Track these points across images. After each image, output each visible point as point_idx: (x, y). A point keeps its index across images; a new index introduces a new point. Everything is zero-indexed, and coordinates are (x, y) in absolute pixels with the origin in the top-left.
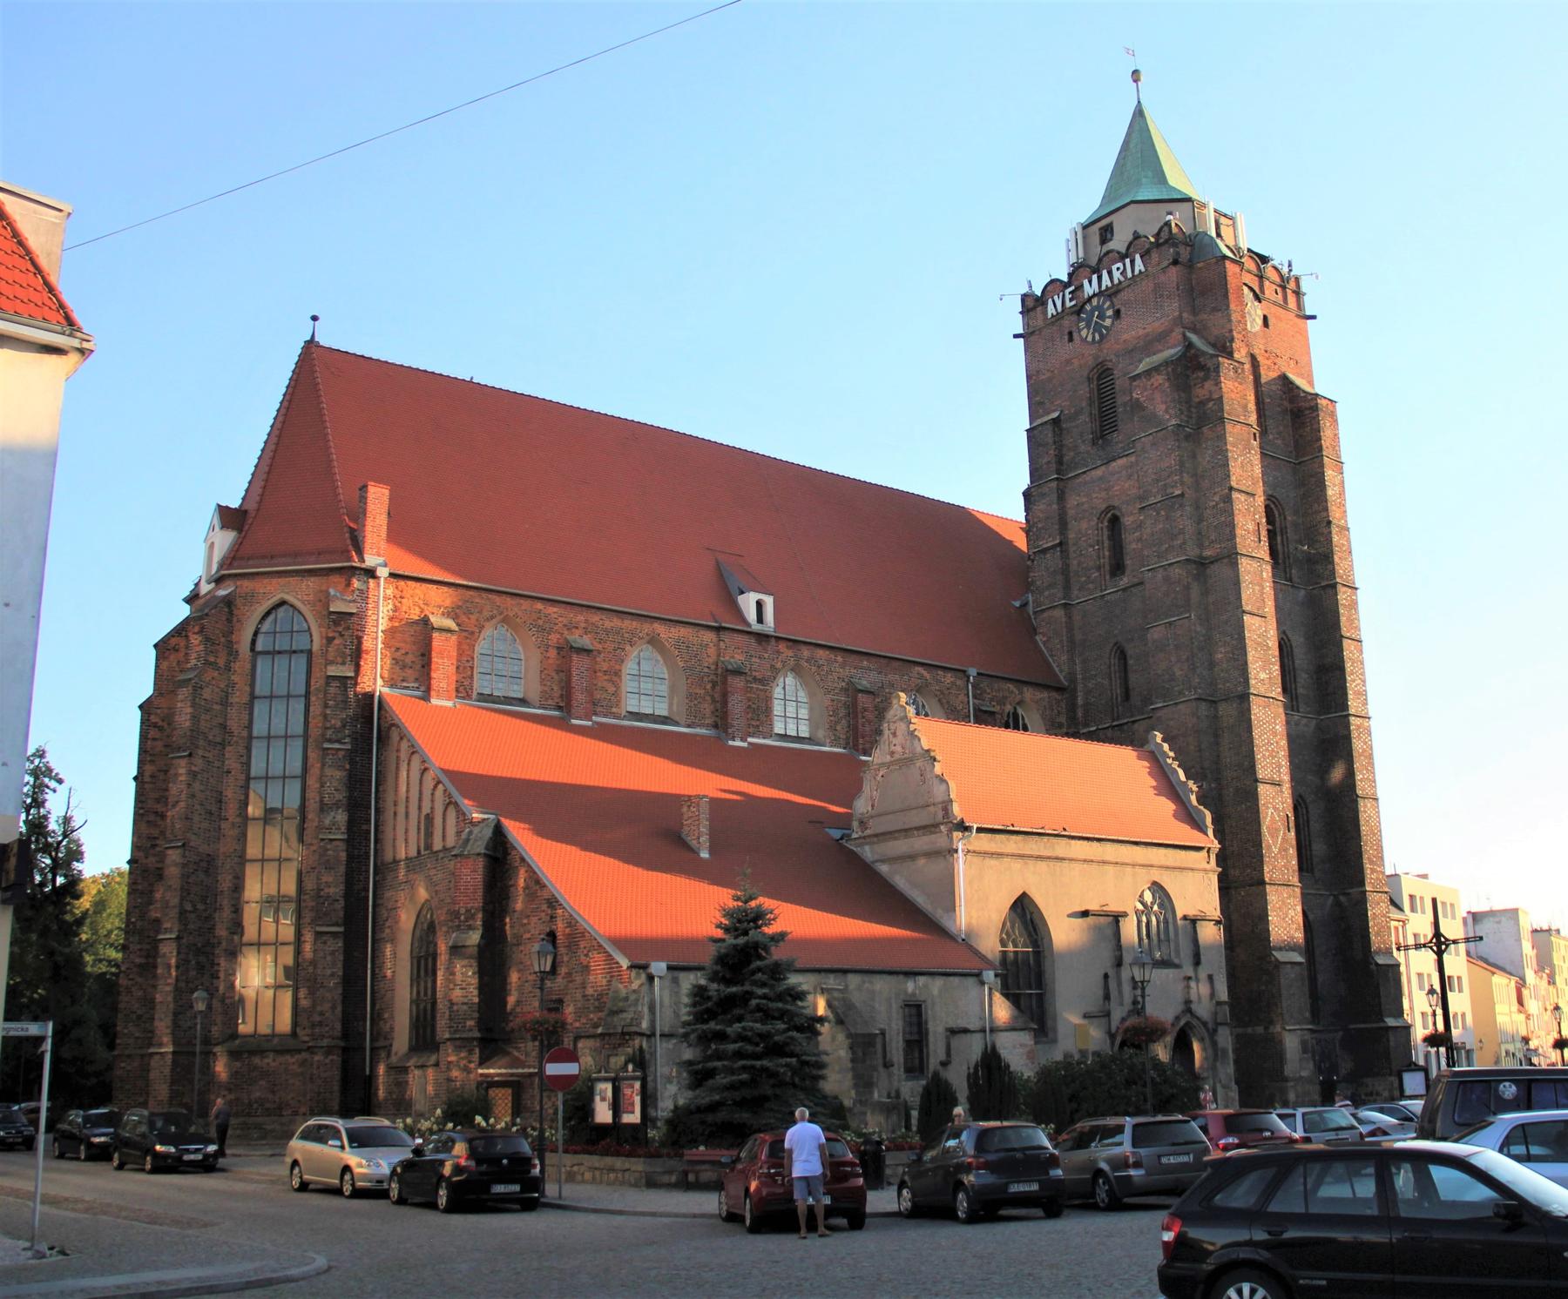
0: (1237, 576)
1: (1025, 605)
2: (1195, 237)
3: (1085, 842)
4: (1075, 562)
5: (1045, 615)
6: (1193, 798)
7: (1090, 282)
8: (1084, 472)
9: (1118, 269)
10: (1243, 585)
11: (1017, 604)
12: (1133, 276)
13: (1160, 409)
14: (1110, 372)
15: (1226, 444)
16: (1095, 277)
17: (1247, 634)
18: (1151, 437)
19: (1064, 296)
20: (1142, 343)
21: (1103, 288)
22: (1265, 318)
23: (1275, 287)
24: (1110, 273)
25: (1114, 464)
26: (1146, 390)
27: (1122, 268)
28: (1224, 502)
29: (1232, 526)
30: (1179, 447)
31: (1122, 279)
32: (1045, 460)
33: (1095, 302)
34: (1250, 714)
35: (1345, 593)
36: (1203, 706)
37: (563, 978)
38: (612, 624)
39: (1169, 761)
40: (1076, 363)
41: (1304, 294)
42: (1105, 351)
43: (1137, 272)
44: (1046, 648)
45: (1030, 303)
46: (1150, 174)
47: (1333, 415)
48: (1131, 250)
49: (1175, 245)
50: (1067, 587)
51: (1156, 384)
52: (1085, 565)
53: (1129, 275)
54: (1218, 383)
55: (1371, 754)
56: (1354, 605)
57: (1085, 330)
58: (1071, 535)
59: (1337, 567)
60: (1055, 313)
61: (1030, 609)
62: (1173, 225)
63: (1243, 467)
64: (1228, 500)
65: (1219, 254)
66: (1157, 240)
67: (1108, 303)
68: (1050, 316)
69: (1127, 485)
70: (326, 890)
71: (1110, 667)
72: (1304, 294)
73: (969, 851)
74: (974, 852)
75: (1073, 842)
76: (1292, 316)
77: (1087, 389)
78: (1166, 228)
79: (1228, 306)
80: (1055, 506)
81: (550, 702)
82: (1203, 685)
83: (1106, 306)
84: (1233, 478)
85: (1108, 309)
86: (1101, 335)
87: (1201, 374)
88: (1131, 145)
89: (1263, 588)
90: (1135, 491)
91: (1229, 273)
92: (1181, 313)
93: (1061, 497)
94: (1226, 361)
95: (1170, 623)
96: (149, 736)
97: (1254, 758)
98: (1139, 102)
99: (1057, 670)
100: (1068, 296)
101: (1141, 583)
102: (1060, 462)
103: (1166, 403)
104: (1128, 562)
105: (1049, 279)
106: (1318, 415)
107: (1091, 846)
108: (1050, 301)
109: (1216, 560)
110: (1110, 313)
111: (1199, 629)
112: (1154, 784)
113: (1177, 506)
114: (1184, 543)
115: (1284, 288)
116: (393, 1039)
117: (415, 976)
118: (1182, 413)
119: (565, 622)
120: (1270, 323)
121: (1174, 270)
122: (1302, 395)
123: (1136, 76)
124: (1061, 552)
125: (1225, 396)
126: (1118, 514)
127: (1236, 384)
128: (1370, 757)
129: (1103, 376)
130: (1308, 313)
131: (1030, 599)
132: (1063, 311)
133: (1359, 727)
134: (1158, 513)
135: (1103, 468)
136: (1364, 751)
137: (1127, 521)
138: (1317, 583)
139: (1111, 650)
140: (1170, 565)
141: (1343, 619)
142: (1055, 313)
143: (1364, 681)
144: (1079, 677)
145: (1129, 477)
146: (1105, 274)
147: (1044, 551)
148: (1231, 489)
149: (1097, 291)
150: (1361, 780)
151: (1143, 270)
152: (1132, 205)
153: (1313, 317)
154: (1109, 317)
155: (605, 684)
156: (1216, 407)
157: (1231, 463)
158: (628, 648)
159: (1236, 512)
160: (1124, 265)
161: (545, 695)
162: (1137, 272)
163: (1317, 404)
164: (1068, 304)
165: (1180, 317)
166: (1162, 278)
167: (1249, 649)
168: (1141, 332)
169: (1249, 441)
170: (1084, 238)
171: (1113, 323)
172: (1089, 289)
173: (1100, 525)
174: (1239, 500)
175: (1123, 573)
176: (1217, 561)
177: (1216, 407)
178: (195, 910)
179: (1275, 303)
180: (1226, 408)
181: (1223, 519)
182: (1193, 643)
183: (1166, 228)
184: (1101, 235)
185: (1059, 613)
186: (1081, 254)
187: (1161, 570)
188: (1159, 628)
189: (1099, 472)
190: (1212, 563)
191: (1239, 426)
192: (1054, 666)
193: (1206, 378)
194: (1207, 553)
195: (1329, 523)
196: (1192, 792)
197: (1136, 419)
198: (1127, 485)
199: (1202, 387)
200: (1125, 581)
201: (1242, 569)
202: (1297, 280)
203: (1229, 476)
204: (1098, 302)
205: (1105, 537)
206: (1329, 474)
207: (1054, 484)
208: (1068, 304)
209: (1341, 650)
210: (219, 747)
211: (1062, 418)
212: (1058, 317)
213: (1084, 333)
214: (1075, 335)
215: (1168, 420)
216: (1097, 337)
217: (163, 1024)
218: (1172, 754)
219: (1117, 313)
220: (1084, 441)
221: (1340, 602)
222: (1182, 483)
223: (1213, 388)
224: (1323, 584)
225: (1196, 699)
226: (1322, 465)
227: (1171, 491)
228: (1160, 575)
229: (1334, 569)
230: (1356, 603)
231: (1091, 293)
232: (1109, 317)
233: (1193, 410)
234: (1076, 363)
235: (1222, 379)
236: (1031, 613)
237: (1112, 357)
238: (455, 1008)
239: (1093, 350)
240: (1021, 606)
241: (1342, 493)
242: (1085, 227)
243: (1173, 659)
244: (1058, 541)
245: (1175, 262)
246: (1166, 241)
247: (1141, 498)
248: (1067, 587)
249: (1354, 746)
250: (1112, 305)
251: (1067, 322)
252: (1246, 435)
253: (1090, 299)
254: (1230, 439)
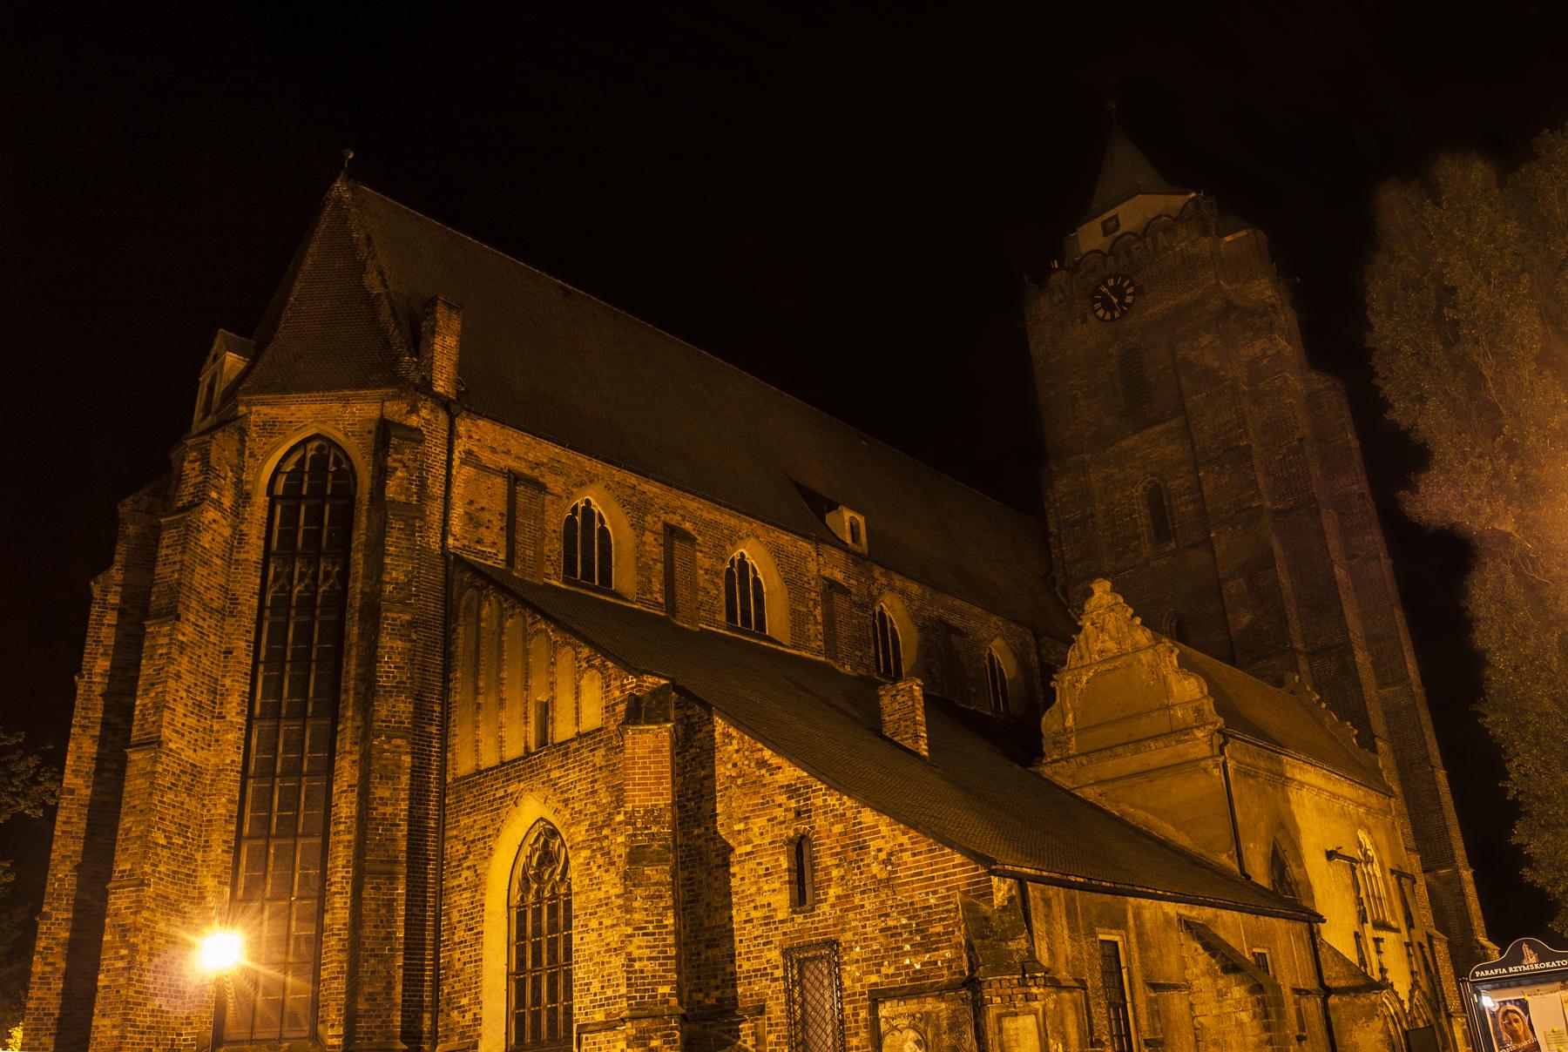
37: (833, 906)
38: (712, 517)
67: (1127, 282)
70: (381, 810)
81: (649, 596)
83: (1125, 285)
85: (1128, 287)
96: (105, 622)
116: (479, 1035)
117: (514, 937)
119: (662, 505)
154: (1130, 294)
155: (706, 585)
158: (729, 547)
161: (645, 587)
178: (170, 845)
210: (217, 616)
214: (1091, 318)
217: (107, 1022)
232: (1130, 294)
238: (637, 965)
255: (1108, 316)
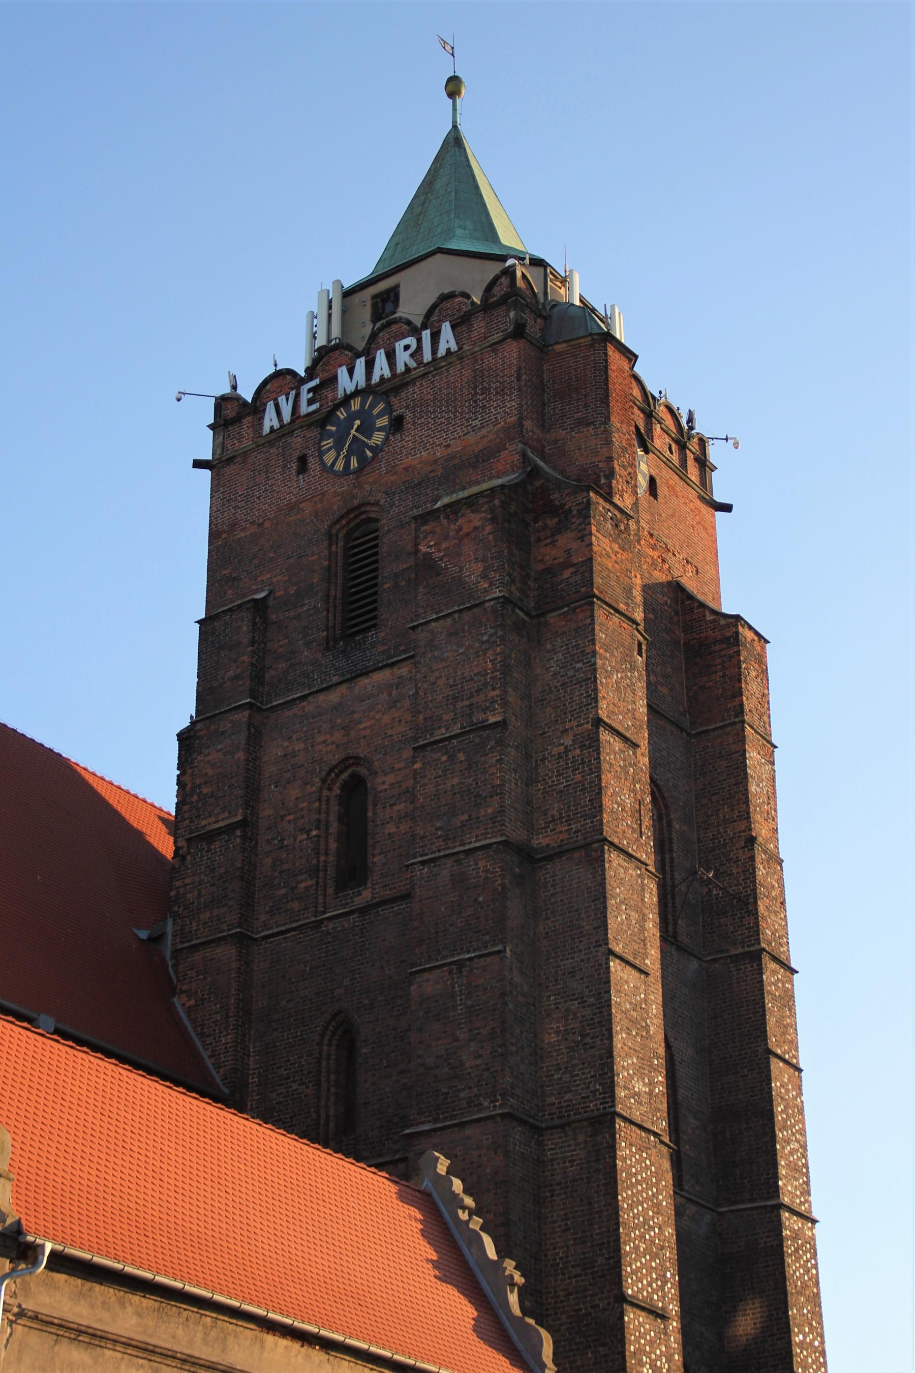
0: (602, 884)
1: (157, 939)
2: (554, 306)
3: (296, 1346)
4: (268, 861)
5: (197, 957)
6: (513, 1298)
7: (351, 372)
8: (303, 698)
9: (407, 348)
10: (611, 902)
11: (143, 935)
12: (434, 359)
13: (472, 571)
14: (373, 526)
15: (593, 642)
16: (360, 363)
17: (614, 999)
18: (449, 621)
19: (298, 396)
20: (440, 471)
21: (376, 379)
22: (652, 481)
23: (668, 440)
24: (391, 357)
25: (365, 681)
26: (446, 538)
27: (414, 346)
28: (583, 746)
29: (597, 791)
30: (502, 639)
31: (412, 364)
32: (231, 673)
33: (356, 405)
34: (614, 1157)
35: (774, 972)
36: (517, 1133)
39: (463, 1216)
40: (307, 507)
41: (713, 469)
42: (367, 487)
43: (442, 352)
44: (193, 1021)
45: (230, 411)
46: (470, 225)
47: (761, 660)
48: (434, 318)
49: (516, 306)
50: (247, 904)
51: (465, 530)
52: (286, 866)
53: (427, 356)
54: (584, 536)
55: (817, 1295)
56: (788, 1000)
57: (333, 453)
58: (266, 812)
59: (762, 923)
60: (276, 425)
61: (168, 948)
62: (519, 274)
63: (618, 689)
64: (592, 744)
65: (598, 331)
66: (485, 299)
67: (381, 406)
68: (266, 429)
69: (386, 718)
71: (319, 1062)
72: (713, 469)
73: (21, 1314)
74: (36, 1317)
75: (270, 1339)
76: (693, 495)
77: (326, 552)
78: (504, 281)
79: (608, 418)
80: (240, 755)
82: (518, 1091)
83: (375, 412)
84: (603, 704)
85: (380, 415)
86: (362, 459)
87: (552, 522)
88: (438, 185)
89: (644, 920)
90: (402, 729)
91: (613, 367)
92: (521, 419)
93: (255, 738)
94: (601, 501)
95: (460, 964)
97: (618, 1249)
98: (455, 127)
99: (209, 1063)
100: (305, 396)
101: (406, 896)
102: (258, 678)
103: (484, 560)
104: (377, 860)
105: (272, 370)
106: (738, 653)
107: (308, 1356)
108: (270, 406)
109: (559, 853)
110: (383, 422)
111: (517, 979)
112: (434, 1257)
113: (492, 743)
114: (501, 812)
115: (683, 447)
118: (513, 581)
120: (662, 490)
121: (513, 351)
122: (709, 617)
123: (453, 87)
124: (244, 838)
125: (597, 559)
126: (363, 771)
127: (616, 547)
128: (815, 1300)
129: (355, 535)
130: (718, 497)
131: (170, 928)
132: (293, 421)
133: (796, 1235)
134: (452, 757)
135: (343, 688)
136: (805, 1286)
137: (382, 783)
138: (722, 951)
139: (326, 1028)
140: (468, 852)
141: (771, 1021)
142: (276, 425)
143: (804, 1147)
144: (253, 1080)
145: (394, 704)
146: (381, 359)
147: (209, 837)
148: (598, 722)
149: (362, 384)
150: (801, 1345)
151: (454, 347)
152: (439, 256)
153: (727, 508)
154: (380, 429)
156: (578, 578)
157: (601, 679)
159: (605, 766)
160: (419, 340)
162: (442, 352)
163: (737, 633)
164: (304, 409)
165: (520, 424)
166: (490, 360)
167: (617, 1028)
168: (439, 453)
169: (631, 650)
170: (344, 312)
171: (387, 439)
172: (346, 383)
173: (325, 793)
174: (609, 742)
175: (363, 882)
176: (560, 854)
177: (578, 578)
179: (668, 463)
180: (598, 580)
181: (578, 777)
182: (505, 1004)
183: (504, 281)
184: (374, 307)
185: (227, 953)
186: (336, 332)
187: (449, 862)
188: (437, 973)
189: (334, 697)
190: (549, 858)
191: (616, 619)
192: (205, 1055)
193: (558, 530)
194: (541, 841)
195: (752, 840)
196: (513, 1285)
197: (421, 589)
198: (386, 718)
199: (553, 543)
200: (366, 896)
201: (610, 873)
202: (702, 442)
203: (596, 700)
204: (363, 404)
205: (333, 817)
206: (753, 756)
207: (243, 716)
208: (304, 409)
209: (767, 1079)
211: (271, 603)
212: (283, 432)
213: (329, 458)
214: (312, 462)
215: (486, 591)
216: (354, 463)
218: (469, 1201)
219: (397, 424)
220: (308, 644)
221: (767, 988)
222: (505, 704)
223: (574, 545)
224: (733, 952)
225: (503, 1116)
226: (742, 740)
227: (482, 716)
228: (445, 873)
229: (757, 924)
230: (792, 997)
231: (350, 388)
232: (380, 429)
233: (531, 583)
234: (307, 507)
235: (593, 529)
236: (168, 956)
237: (380, 496)
239: (344, 485)
240: (150, 939)
241: (772, 797)
242: (348, 294)
243: (462, 1035)
244: (240, 818)
245: (519, 332)
246: (503, 301)
247: (415, 739)
248: (247, 904)
249: (790, 1271)
250: (389, 409)
251: (297, 441)
252: (627, 640)
253: (348, 398)
254: (601, 636)
255: (339, 466)
